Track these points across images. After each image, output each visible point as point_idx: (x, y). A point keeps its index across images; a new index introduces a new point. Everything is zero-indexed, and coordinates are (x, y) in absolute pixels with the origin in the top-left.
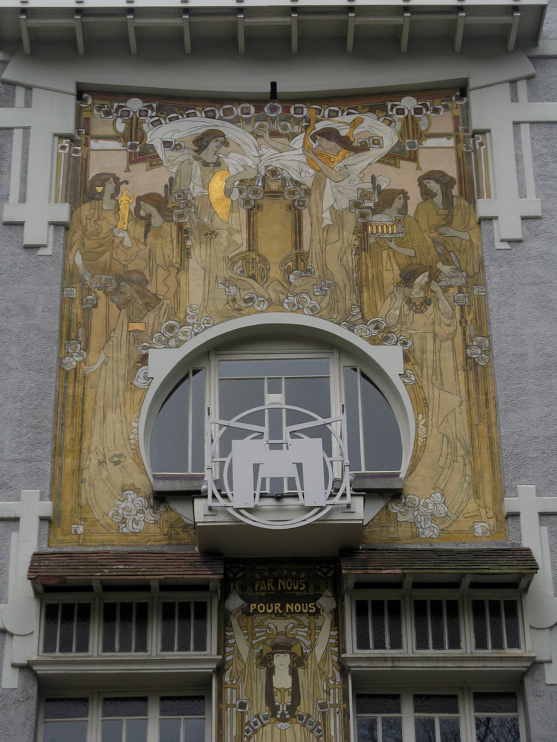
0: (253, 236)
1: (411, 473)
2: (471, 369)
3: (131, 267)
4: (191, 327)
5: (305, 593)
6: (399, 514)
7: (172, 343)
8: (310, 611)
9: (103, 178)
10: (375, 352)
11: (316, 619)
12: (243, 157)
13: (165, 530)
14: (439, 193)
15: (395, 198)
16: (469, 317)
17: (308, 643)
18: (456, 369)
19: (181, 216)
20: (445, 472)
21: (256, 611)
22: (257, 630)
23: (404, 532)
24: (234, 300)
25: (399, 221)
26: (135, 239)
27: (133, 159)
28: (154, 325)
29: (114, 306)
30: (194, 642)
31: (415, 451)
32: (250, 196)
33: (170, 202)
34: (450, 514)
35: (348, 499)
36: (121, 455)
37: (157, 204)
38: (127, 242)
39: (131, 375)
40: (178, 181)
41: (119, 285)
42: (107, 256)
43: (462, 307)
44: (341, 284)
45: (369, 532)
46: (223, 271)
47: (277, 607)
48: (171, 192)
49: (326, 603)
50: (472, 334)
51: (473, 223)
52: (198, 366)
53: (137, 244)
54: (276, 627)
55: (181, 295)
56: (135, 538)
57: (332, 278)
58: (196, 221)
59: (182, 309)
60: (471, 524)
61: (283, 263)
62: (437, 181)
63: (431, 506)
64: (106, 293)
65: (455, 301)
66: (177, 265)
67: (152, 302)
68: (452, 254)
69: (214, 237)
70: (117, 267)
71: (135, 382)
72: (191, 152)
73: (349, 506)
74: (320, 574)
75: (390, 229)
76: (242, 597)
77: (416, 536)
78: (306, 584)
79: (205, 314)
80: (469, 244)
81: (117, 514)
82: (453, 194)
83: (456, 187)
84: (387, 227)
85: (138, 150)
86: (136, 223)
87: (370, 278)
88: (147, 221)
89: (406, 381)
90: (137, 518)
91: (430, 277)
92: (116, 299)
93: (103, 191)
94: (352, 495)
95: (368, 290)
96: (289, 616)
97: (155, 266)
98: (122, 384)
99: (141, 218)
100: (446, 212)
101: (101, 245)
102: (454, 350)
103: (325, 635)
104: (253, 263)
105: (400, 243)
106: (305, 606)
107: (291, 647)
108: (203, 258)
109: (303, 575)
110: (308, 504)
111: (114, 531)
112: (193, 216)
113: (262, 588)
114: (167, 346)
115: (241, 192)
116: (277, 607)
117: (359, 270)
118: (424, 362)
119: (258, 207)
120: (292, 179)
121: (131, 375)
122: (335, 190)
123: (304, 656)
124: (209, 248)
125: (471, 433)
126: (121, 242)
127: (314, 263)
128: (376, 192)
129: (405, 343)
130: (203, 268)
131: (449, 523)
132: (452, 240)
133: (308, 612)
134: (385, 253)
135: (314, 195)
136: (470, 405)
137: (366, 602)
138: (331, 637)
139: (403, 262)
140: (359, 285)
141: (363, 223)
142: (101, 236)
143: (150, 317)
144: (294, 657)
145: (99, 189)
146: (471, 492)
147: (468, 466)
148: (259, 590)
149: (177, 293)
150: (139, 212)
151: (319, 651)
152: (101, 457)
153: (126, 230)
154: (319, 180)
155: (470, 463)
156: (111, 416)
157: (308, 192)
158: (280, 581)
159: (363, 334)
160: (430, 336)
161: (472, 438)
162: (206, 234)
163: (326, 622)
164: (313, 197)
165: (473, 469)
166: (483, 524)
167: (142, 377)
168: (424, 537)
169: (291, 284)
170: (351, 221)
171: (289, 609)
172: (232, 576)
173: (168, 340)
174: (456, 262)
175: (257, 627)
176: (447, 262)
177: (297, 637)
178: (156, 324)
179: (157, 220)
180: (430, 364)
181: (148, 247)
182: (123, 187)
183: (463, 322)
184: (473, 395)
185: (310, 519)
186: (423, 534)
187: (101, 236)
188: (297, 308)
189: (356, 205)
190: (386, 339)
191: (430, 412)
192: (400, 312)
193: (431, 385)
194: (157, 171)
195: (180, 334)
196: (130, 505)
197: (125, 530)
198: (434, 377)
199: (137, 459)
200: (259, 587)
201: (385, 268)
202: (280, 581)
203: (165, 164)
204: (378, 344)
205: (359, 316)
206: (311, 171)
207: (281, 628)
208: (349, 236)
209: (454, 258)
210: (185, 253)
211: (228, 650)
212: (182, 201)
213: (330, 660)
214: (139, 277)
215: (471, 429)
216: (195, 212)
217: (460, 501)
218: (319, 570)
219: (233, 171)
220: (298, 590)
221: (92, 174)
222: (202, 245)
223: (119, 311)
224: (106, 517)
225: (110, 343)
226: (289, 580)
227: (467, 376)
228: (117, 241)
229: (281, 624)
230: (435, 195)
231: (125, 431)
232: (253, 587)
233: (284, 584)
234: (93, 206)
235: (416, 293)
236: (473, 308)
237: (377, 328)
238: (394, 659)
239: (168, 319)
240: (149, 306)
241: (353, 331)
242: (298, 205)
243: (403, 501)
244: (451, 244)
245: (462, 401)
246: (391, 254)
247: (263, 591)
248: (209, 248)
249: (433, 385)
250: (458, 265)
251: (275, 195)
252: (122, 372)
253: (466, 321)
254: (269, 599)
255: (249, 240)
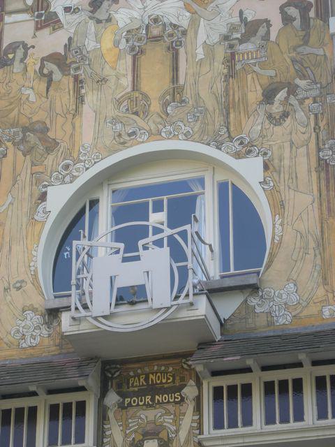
0: (137, 77)
1: (267, 270)
2: (323, 170)
3: (35, 119)
4: (83, 164)
5: (172, 385)
6: (256, 307)
7: (67, 179)
8: (176, 400)
9: (14, 46)
10: (241, 166)
11: (181, 408)
12: (130, 11)
13: (58, 341)
14: (298, 17)
15: (259, 27)
16: (322, 124)
17: (173, 428)
18: (309, 171)
19: (77, 69)
20: (298, 264)
21: (130, 405)
22: (130, 421)
23: (261, 322)
24: (120, 135)
25: (263, 47)
26: (39, 95)
27: (39, 26)
28: (52, 165)
29: (20, 153)
30: (76, 437)
31: (272, 249)
32: (135, 43)
33: (68, 59)
34: (301, 301)
35: (191, 298)
36: (23, 281)
37: (58, 61)
38: (32, 98)
39: (33, 210)
40: (75, 39)
41: (24, 135)
42: (16, 112)
43: (316, 115)
44: (211, 109)
45: (232, 325)
46: (111, 111)
47: (148, 399)
48: (69, 50)
49: (190, 391)
50: (325, 138)
51: (327, 39)
52: (94, 197)
53: (40, 98)
54: (147, 417)
55: (76, 137)
56: (32, 351)
57: (202, 105)
58: (89, 71)
59: (76, 148)
60: (319, 308)
61: (163, 96)
62: (296, 7)
63: (284, 296)
64: (14, 144)
65: (310, 110)
66: (72, 112)
67: (51, 146)
68: (308, 69)
69: (103, 83)
70: (24, 121)
71: (36, 217)
72: (87, 13)
73: (192, 304)
74: (185, 366)
75: (254, 55)
76: (119, 393)
77: (270, 324)
78: (174, 376)
79: (95, 151)
80: (323, 58)
81: (18, 331)
82: (310, 16)
83: (313, 10)
84: (252, 53)
85: (43, 18)
86: (40, 81)
87: (237, 100)
88: (49, 79)
89: (265, 187)
90: (34, 334)
91: (289, 93)
92: (22, 147)
93: (14, 57)
94: (194, 295)
95: (234, 111)
96: (158, 406)
97: (54, 114)
98: (25, 220)
99: (45, 75)
100: (304, 33)
101: (11, 103)
102: (308, 154)
103: (188, 419)
104: (136, 101)
105: (263, 66)
106: (171, 396)
107: (158, 434)
108: (95, 102)
109: (171, 369)
110: (155, 306)
111: (15, 347)
112: (87, 68)
113: (135, 384)
114: (63, 182)
115: (127, 41)
116: (148, 399)
117: (227, 94)
118: (282, 168)
119: (142, 52)
120: (171, 24)
121: (33, 210)
122: (208, 28)
123: (170, 440)
124: (99, 93)
125: (322, 227)
126: (27, 99)
127: (188, 94)
128: (243, 24)
129: (265, 154)
130: (94, 111)
131: (300, 310)
132: (308, 58)
133: (174, 401)
134: (249, 77)
135: (190, 34)
136: (321, 202)
137: (222, 387)
138: (193, 421)
139: (265, 81)
140: (226, 109)
141: (231, 53)
142: (11, 95)
143: (50, 160)
144: (161, 442)
145: (11, 56)
146: (321, 280)
147: (319, 257)
148: (133, 386)
149: (72, 135)
150: (43, 70)
151: (183, 435)
152: (6, 285)
153: (32, 88)
154: (194, 23)
155: (320, 254)
156: (15, 248)
157: (184, 33)
158: (151, 376)
159: (229, 150)
160: (287, 145)
161: (322, 232)
162: (98, 82)
163: (190, 408)
164: (188, 36)
165: (323, 259)
166: (329, 307)
167: (41, 212)
168: (278, 324)
169: (168, 114)
170: (221, 53)
171: (158, 401)
172: (110, 376)
173: (64, 178)
174: (312, 76)
175: (130, 419)
176: (303, 77)
177: (165, 424)
178: (55, 163)
179: (57, 75)
180: (286, 169)
181: (49, 100)
182: (30, 51)
183: (317, 128)
184: (324, 192)
185: (157, 318)
186: (277, 321)
187: (11, 95)
188: (172, 136)
189: (226, 38)
190: (249, 152)
191: (286, 213)
192: (262, 127)
193: (287, 188)
194: (60, 33)
195: (74, 171)
196: (28, 323)
197: (24, 345)
198: (290, 181)
199: (35, 282)
200: (133, 383)
201: (249, 90)
202: (151, 376)
203: (65, 27)
204: (243, 158)
205: (227, 135)
206: (188, 14)
207: (151, 418)
208: (220, 67)
209: (310, 72)
210: (80, 100)
211: (105, 441)
212: (79, 56)
213: (192, 442)
214: (41, 126)
215: (322, 223)
216: (89, 65)
217: (310, 288)
218: (184, 363)
219: (121, 24)
220: (166, 383)
221: (5, 45)
222: (94, 91)
223: (24, 158)
224: (9, 335)
225: (16, 186)
226: (159, 374)
227: (319, 176)
228: (24, 98)
229: (150, 415)
230: (294, 19)
231: (26, 259)
232: (128, 384)
233: (154, 378)
234: (6, 71)
235: (276, 108)
236: (325, 115)
237: (241, 143)
238: (243, 436)
239: (65, 159)
240: (49, 150)
241: (220, 149)
242: (176, 46)
243: (260, 294)
244: (308, 61)
245: (314, 199)
246: (255, 76)
247: (136, 386)
248: (99, 93)
249: (289, 188)
250: (313, 79)
251: (156, 39)
252: (25, 210)
253: (320, 127)
254: (141, 393)
255: (134, 82)
